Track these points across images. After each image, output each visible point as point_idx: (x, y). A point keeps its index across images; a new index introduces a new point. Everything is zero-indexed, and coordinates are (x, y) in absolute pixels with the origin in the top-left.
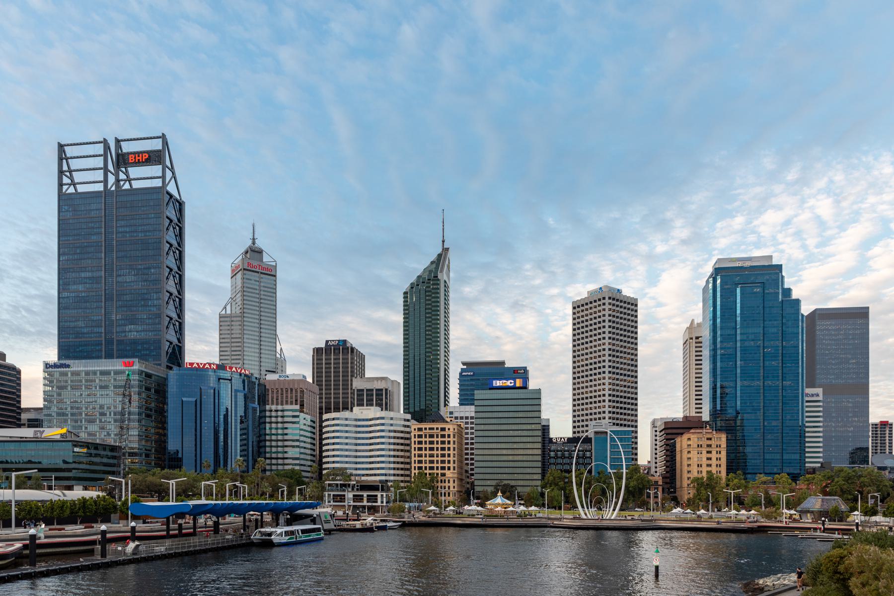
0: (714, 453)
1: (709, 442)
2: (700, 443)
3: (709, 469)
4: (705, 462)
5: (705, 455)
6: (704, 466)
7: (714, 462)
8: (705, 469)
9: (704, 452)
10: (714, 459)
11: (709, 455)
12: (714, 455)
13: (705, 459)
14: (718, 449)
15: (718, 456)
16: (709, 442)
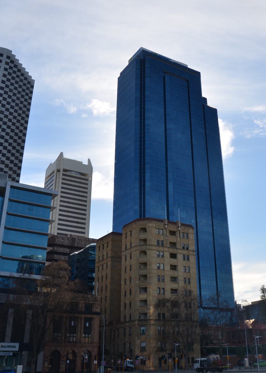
0: (180, 257)
1: (172, 239)
2: (161, 238)
3: (175, 286)
4: (168, 273)
5: (168, 261)
6: (167, 279)
7: (180, 273)
8: (169, 285)
9: (167, 255)
10: (181, 269)
11: (173, 261)
12: (180, 261)
13: (168, 268)
14: (185, 252)
15: (186, 263)
16: (172, 239)
